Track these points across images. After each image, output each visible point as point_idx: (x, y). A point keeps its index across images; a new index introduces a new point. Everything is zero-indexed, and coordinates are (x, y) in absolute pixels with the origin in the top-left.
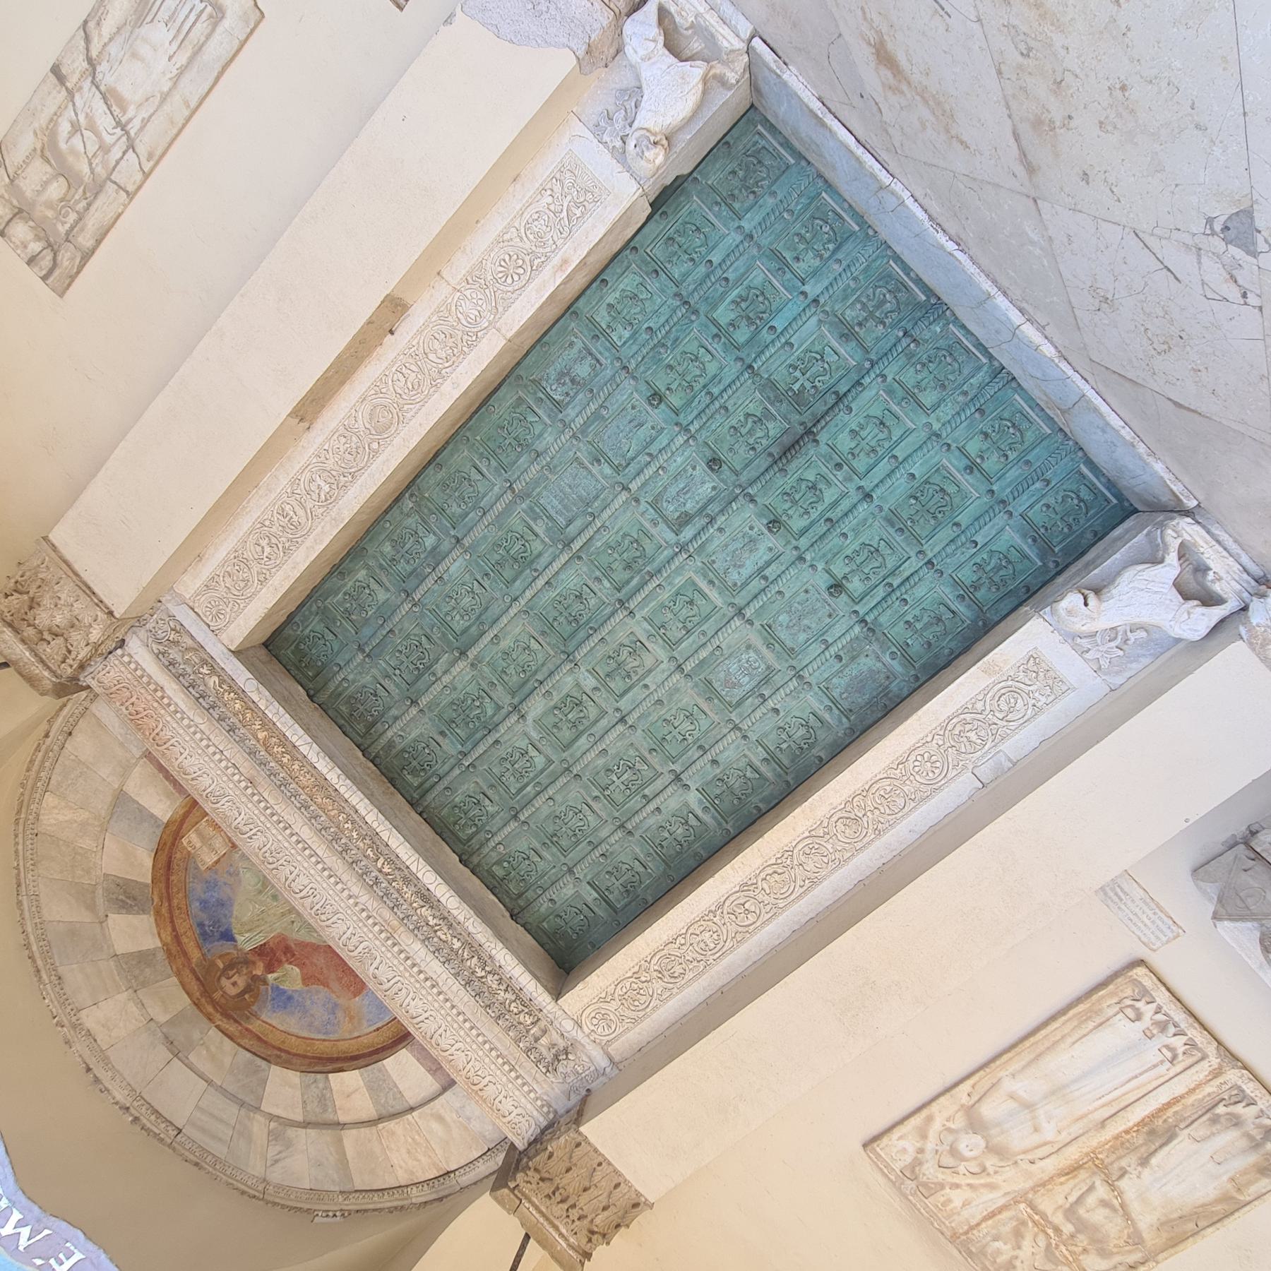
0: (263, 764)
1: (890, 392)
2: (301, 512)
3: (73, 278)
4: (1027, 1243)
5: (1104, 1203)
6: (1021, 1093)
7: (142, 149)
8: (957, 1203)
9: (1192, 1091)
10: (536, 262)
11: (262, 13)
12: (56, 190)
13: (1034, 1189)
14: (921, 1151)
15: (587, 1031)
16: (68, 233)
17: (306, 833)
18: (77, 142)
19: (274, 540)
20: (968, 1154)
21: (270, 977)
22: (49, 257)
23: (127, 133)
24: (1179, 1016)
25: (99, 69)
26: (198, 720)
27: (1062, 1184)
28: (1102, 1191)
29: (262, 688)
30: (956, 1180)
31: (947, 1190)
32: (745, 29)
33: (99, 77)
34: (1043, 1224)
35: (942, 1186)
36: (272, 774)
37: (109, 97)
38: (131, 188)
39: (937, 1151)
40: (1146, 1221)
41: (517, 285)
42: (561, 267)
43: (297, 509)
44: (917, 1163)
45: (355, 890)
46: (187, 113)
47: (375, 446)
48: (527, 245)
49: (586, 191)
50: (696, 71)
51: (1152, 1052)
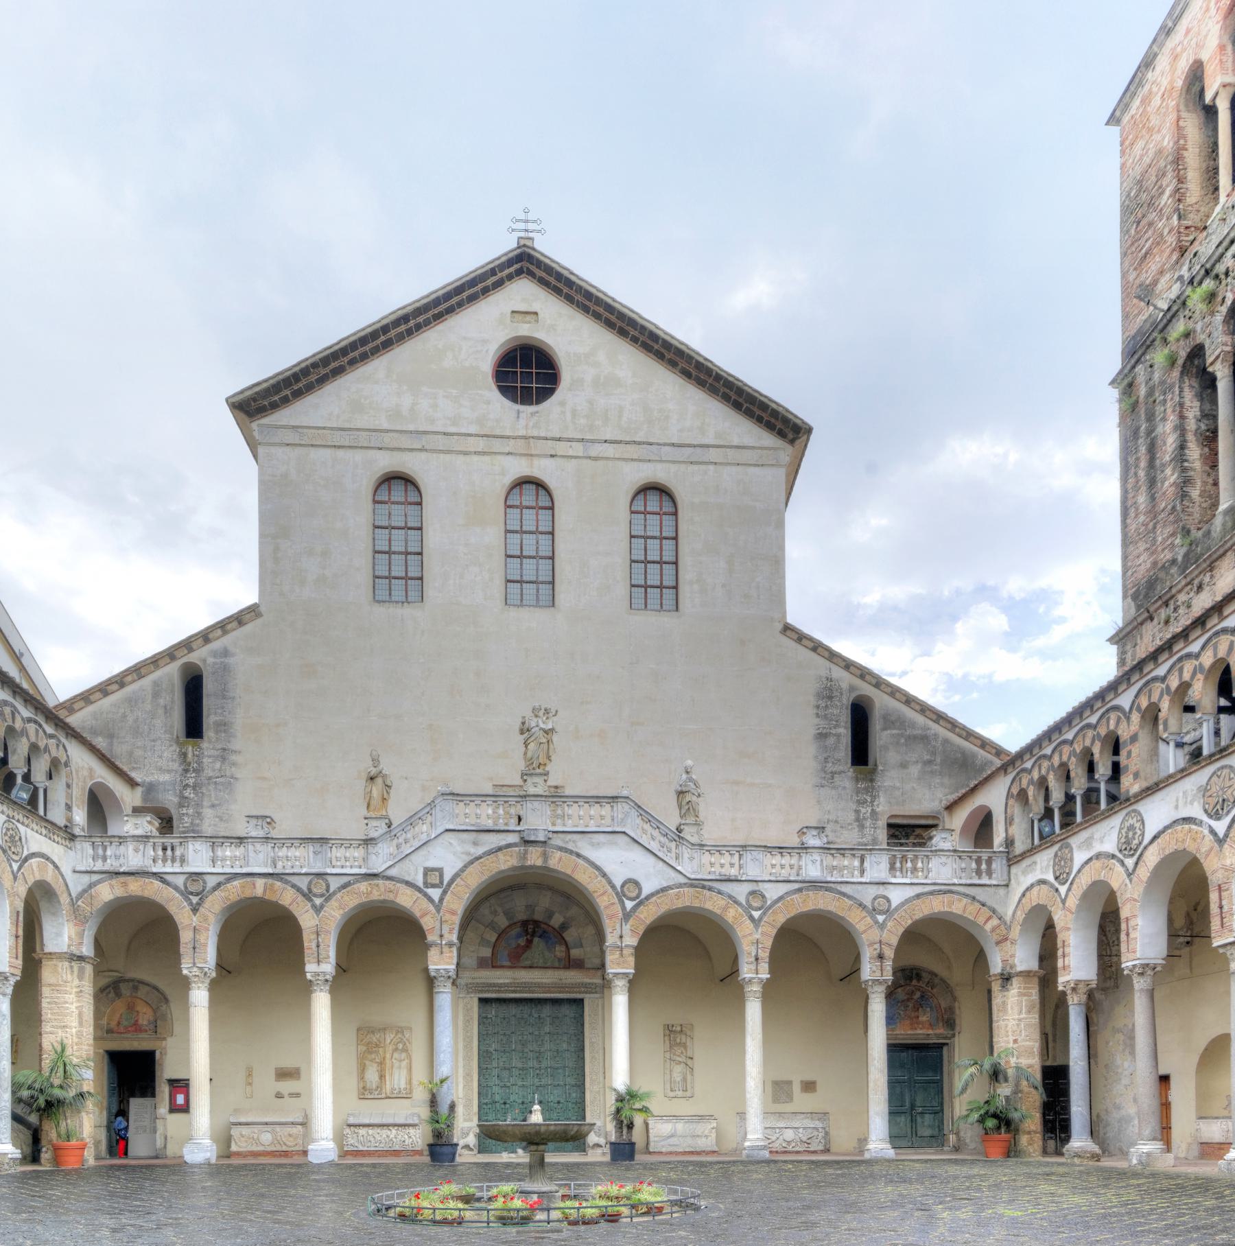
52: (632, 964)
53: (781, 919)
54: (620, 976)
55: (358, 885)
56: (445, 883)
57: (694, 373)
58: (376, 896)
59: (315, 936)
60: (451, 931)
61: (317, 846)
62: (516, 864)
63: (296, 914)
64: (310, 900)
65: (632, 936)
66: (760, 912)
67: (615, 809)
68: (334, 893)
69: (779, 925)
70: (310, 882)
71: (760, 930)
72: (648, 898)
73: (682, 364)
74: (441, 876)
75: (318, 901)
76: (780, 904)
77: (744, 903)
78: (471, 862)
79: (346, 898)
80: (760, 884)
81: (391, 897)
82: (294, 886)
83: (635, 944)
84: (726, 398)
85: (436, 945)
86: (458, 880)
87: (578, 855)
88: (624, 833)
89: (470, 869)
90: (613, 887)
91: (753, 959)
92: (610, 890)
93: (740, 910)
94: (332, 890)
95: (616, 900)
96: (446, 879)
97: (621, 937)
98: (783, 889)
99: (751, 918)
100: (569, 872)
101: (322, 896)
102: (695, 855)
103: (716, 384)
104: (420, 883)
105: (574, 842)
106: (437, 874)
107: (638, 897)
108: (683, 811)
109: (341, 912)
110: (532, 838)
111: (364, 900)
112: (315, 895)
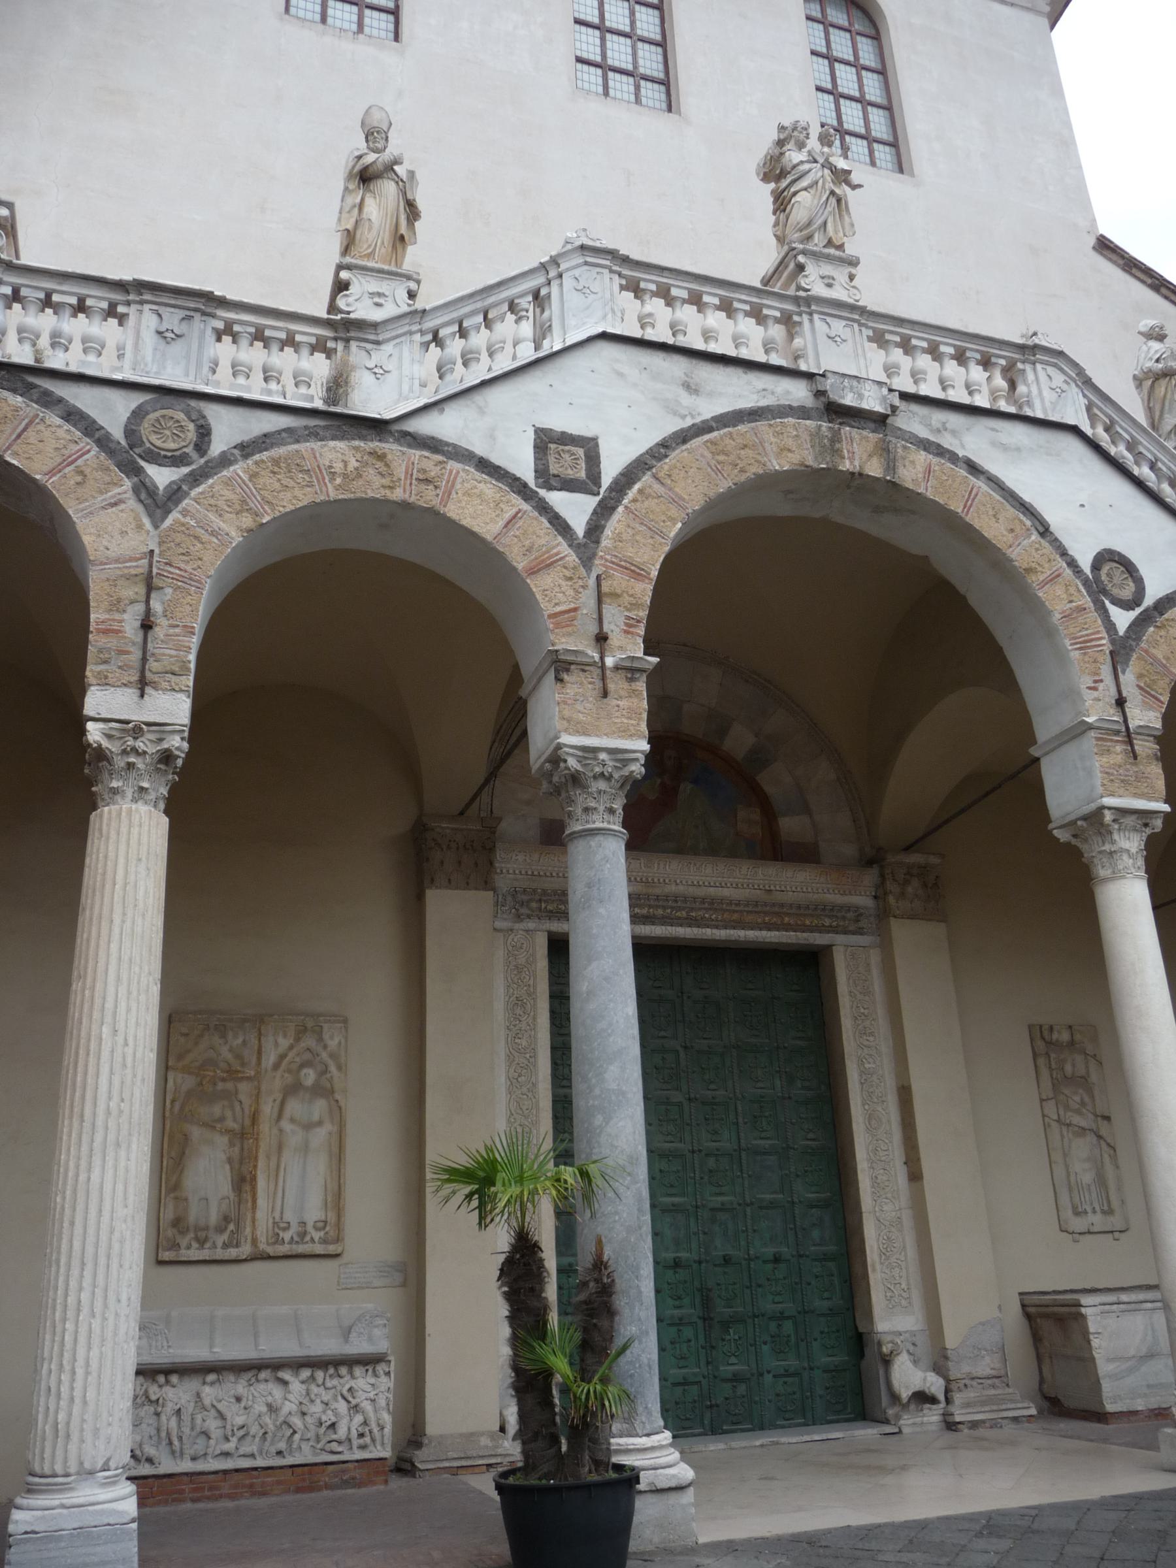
0: (774, 905)
1: (695, 1375)
2: (866, 1043)
3: (1032, 1040)
4: (229, 1057)
5: (222, 1119)
6: (318, 1130)
7: (1054, 1125)
8: (281, 1040)
9: (254, 1221)
10: (883, 1257)
11: (1062, 1231)
12: (1068, 1068)
13: (259, 1088)
14: (325, 1047)
15: (521, 932)
16: (1049, 1057)
17: (726, 892)
18: (1077, 1098)
19: (863, 1017)
20: (305, 1071)
21: (659, 781)
22: (1046, 1037)
23: (1064, 1124)
24: (301, 1249)
25: (1095, 1138)
26: (816, 896)
27: (251, 1106)
28: (230, 1124)
29: (806, 942)
30: (295, 1051)
31: (291, 1041)
32: (906, 1430)
33: (1093, 1135)
34: (232, 1075)
35: (298, 1039)
36: (765, 904)
37: (1083, 1131)
38: (1044, 1103)
39: (318, 1055)
40: (196, 1132)
41: (881, 1238)
42: (873, 1266)
43: (867, 1043)
44: (320, 1039)
45: (681, 888)
46: (1052, 1158)
47: (867, 1107)
48: (893, 1259)
49: (894, 1307)
50: (905, 1395)
51: (289, 1216)
52: (1161, 784)
54: (1130, 821)
55: (315, 445)
56: (606, 480)
58: (373, 486)
59: (141, 589)
60: (630, 624)
61: (172, 319)
62: (810, 461)
63: (72, 509)
64: (132, 470)
65: (1146, 706)
67: (1030, 376)
68: (225, 461)
70: (138, 414)
74: (593, 459)
75: (161, 476)
78: (683, 437)
79: (266, 479)
81: (429, 497)
82: (73, 416)
85: (584, 667)
86: (647, 478)
87: (973, 468)
88: (1075, 430)
89: (678, 455)
90: (1072, 564)
92: (1068, 572)
94: (217, 447)
95: (1087, 601)
96: (609, 472)
97: (1120, 702)
100: (956, 506)
101: (177, 460)
104: (527, 473)
105: (954, 433)
106: (580, 452)
109: (247, 521)
110: (849, 400)
111: (333, 495)
112: (155, 457)
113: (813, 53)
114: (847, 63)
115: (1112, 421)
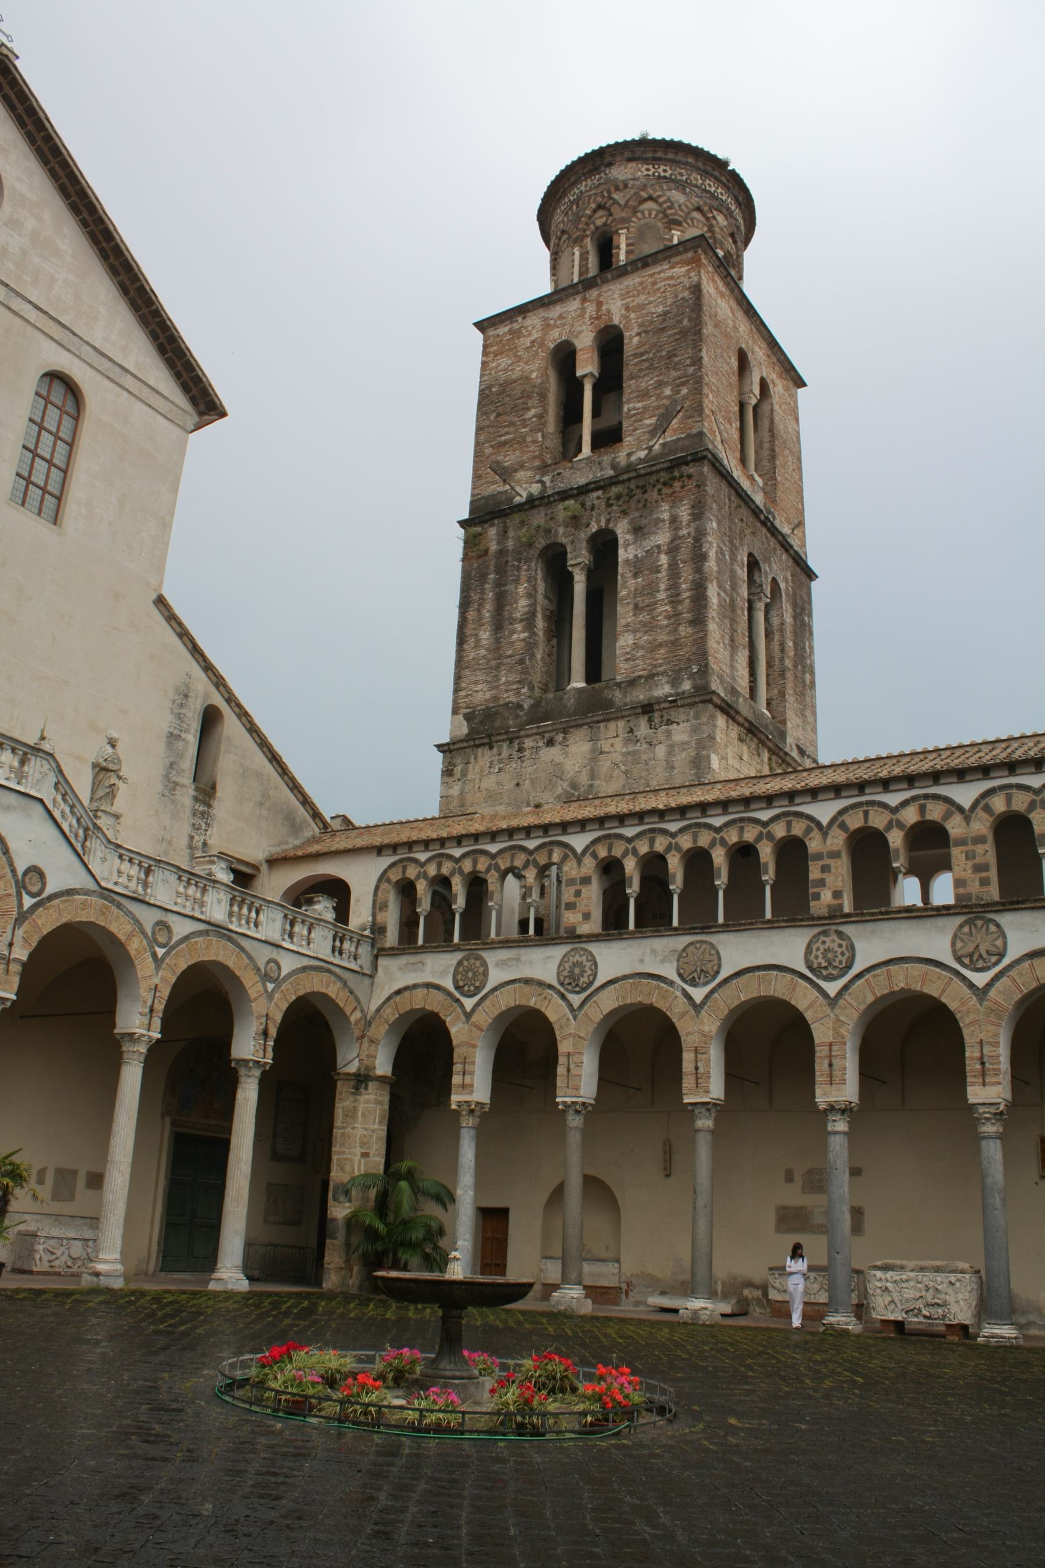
52: (16, 987)
53: (183, 966)
57: (132, 293)
65: (24, 947)
66: (163, 950)
67: (32, 763)
69: (179, 971)
71: (160, 974)
72: (51, 898)
73: (123, 277)
76: (184, 946)
77: (150, 934)
80: (169, 914)
83: (25, 958)
84: (154, 336)
88: (41, 801)
90: (14, 871)
91: (147, 1010)
92: (10, 875)
93: (145, 942)
95: (13, 891)
97: (11, 945)
98: (190, 927)
99: (154, 954)
102: (109, 857)
103: (150, 319)
107: (39, 894)
108: (100, 793)
113: (24, 447)
114: (51, 433)
115: (66, 793)
